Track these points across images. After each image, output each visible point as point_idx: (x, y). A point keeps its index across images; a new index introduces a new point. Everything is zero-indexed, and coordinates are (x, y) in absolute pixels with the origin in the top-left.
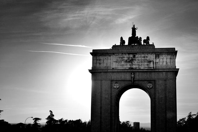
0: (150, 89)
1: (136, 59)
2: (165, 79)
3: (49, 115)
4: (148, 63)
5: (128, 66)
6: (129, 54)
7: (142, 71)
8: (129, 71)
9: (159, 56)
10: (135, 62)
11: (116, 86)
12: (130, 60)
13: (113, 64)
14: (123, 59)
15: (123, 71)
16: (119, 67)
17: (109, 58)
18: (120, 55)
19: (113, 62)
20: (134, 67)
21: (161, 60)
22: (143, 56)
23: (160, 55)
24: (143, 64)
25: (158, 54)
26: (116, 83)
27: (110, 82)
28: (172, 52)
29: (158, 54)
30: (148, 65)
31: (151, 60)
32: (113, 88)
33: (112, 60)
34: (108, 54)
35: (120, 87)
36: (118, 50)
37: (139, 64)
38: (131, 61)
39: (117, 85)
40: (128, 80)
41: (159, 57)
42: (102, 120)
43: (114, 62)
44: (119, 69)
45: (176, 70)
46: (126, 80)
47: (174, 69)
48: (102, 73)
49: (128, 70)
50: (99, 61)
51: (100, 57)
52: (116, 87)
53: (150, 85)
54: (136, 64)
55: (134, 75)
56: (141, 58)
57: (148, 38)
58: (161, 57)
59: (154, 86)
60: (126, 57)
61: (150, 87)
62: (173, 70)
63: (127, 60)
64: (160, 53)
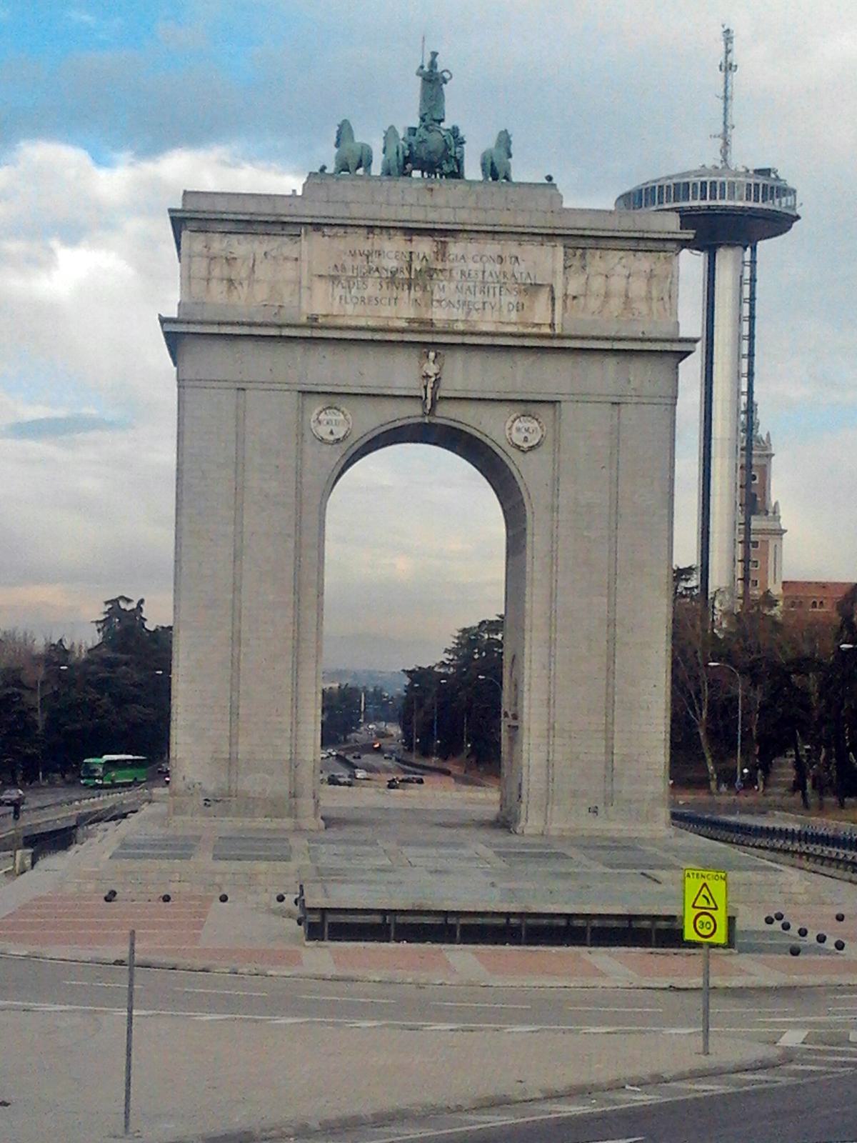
2: (616, 400)
6: (411, 232)
9: (583, 256)
10: (445, 289)
14: (375, 260)
15: (378, 336)
16: (350, 309)
19: (316, 279)
20: (439, 315)
21: (597, 284)
22: (492, 248)
24: (491, 299)
25: (582, 243)
30: (520, 307)
32: (308, 437)
35: (356, 436)
39: (337, 422)
41: (584, 267)
44: (353, 323)
46: (389, 392)
48: (248, 346)
49: (402, 331)
50: (226, 269)
52: (332, 433)
53: (527, 430)
54: (454, 300)
56: (478, 266)
57: (505, 141)
59: (550, 437)
60: (392, 250)
61: (526, 439)
62: (668, 347)
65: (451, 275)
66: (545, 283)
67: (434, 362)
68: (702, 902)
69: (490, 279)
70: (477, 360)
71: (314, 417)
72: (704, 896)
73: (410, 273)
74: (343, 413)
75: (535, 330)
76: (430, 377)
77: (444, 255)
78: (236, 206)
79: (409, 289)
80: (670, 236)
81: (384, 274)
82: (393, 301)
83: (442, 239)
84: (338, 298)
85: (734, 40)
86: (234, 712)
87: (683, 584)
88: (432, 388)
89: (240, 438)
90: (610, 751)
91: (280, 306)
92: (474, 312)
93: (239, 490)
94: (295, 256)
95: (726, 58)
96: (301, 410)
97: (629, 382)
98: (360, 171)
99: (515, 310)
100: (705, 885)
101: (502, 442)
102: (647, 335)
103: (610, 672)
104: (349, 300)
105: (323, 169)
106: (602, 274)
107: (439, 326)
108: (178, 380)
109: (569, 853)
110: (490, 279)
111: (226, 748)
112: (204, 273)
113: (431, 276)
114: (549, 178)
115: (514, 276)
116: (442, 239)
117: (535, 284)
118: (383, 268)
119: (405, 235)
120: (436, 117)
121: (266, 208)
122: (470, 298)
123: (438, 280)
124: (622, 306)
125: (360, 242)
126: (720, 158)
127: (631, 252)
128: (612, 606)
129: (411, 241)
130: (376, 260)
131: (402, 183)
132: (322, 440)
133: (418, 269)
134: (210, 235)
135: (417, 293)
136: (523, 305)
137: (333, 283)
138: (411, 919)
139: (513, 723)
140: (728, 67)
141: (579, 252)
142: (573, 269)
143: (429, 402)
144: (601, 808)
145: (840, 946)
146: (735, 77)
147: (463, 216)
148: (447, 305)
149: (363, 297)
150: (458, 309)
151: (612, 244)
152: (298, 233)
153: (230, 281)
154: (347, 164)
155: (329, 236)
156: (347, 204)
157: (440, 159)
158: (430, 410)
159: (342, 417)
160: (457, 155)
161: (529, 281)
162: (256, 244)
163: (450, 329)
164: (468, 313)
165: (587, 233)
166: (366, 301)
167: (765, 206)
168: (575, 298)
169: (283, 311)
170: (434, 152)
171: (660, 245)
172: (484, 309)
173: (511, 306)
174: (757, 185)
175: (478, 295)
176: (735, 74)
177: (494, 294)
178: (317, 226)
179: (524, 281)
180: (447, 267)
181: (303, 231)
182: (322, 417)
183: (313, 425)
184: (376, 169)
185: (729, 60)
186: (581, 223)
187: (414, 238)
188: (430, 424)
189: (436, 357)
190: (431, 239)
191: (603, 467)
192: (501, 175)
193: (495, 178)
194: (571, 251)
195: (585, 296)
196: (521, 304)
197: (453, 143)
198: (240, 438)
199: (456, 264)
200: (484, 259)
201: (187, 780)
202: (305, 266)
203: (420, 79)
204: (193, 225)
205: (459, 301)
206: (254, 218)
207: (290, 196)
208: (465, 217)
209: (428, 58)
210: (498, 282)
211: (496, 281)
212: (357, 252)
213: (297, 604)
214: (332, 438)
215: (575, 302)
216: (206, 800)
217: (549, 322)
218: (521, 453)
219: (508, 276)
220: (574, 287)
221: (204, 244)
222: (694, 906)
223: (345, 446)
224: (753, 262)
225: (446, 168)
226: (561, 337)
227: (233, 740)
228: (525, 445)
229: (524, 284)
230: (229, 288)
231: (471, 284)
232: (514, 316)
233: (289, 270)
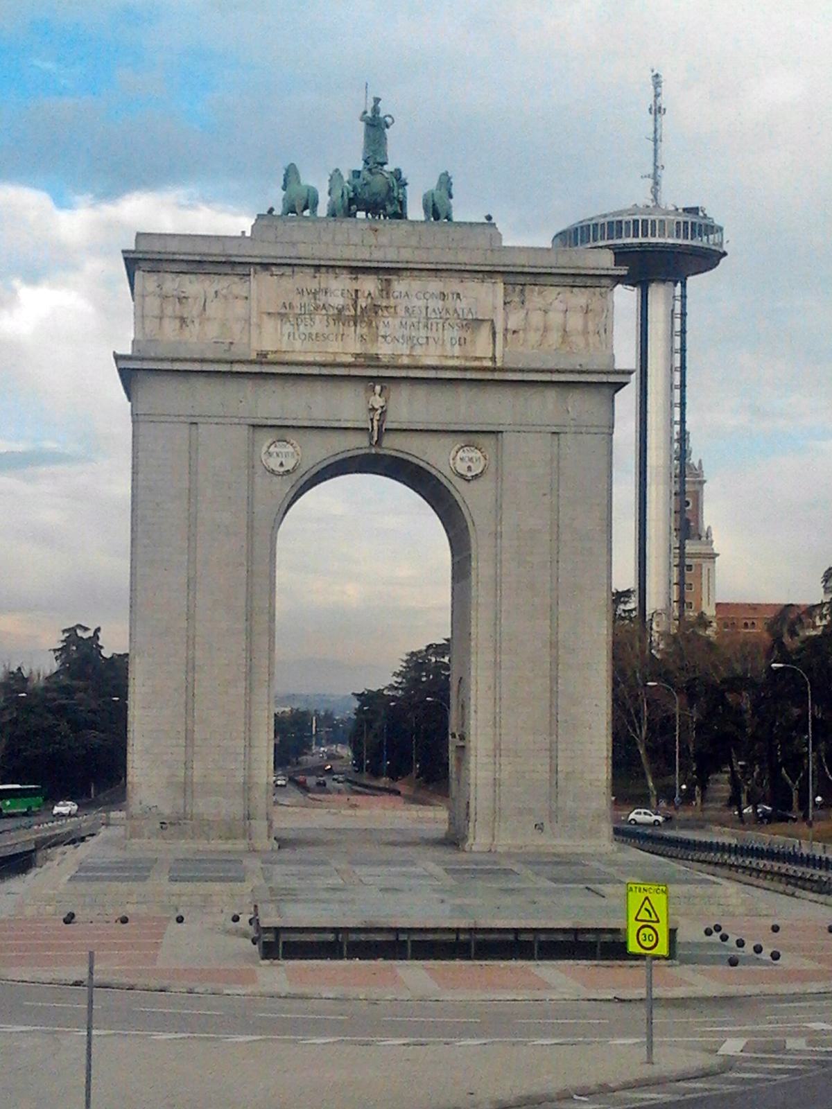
0: (469, 481)
2: (555, 429)
6: (357, 271)
9: (522, 291)
10: (389, 325)
13: (259, 326)
14: (321, 296)
15: (325, 371)
16: (298, 345)
19: (265, 317)
20: (384, 350)
21: (536, 319)
22: (435, 285)
25: (522, 279)
27: (244, 432)
30: (462, 342)
31: (480, 318)
32: (260, 470)
39: (287, 455)
41: (523, 303)
42: (198, 654)
43: (269, 314)
44: (301, 358)
45: (612, 379)
46: (336, 424)
48: (200, 383)
52: (281, 464)
53: (471, 460)
54: (398, 334)
56: (422, 303)
57: (446, 182)
59: (492, 469)
60: (338, 289)
61: (469, 468)
62: (604, 378)
65: (396, 312)
66: (487, 318)
67: (380, 395)
68: (644, 915)
69: (433, 316)
70: (421, 392)
71: (264, 449)
72: (646, 910)
73: (355, 310)
74: (292, 445)
75: (477, 364)
76: (377, 410)
77: (387, 293)
78: (187, 247)
79: (355, 325)
81: (331, 312)
82: (340, 337)
83: (386, 277)
84: (286, 337)
85: (663, 84)
86: (189, 734)
87: (622, 607)
88: (378, 420)
91: (231, 343)
92: (418, 347)
94: (245, 295)
95: (655, 102)
96: (252, 443)
98: (307, 213)
99: (457, 345)
100: (647, 898)
101: (448, 473)
102: (584, 368)
103: (554, 692)
104: (297, 336)
105: (271, 210)
106: (540, 309)
107: (385, 360)
108: (132, 415)
109: (515, 869)
110: (433, 316)
112: (157, 312)
113: (376, 313)
114: (489, 218)
115: (455, 311)
116: (386, 277)
117: (477, 320)
118: (330, 305)
119: (352, 273)
120: (379, 160)
121: (216, 249)
123: (382, 316)
124: (560, 340)
125: (306, 280)
126: (652, 197)
127: (568, 288)
130: (324, 297)
131: (347, 224)
132: (273, 472)
133: (364, 305)
134: (161, 274)
135: (362, 329)
136: (465, 339)
137: (282, 320)
138: (363, 937)
139: (461, 744)
140: (657, 111)
141: (518, 288)
142: (513, 304)
144: (547, 826)
145: (775, 956)
146: (664, 119)
147: (406, 254)
148: (392, 341)
150: (403, 344)
152: (248, 273)
153: (183, 320)
154: (294, 206)
155: (277, 275)
156: (294, 244)
157: (383, 200)
158: (377, 441)
159: (290, 449)
160: (401, 196)
163: (395, 364)
165: (526, 270)
166: (314, 337)
167: (694, 243)
168: (514, 332)
169: (233, 348)
170: (378, 194)
171: (595, 282)
172: (427, 343)
173: (454, 342)
174: (686, 223)
175: (421, 330)
176: (664, 117)
177: (437, 330)
178: (266, 266)
179: (465, 317)
180: (392, 305)
181: (252, 270)
182: (272, 449)
184: (322, 210)
185: (658, 104)
186: (521, 260)
187: (359, 276)
188: (377, 455)
189: (382, 391)
190: (376, 277)
191: (545, 495)
192: (443, 216)
193: (437, 218)
194: (510, 287)
195: (525, 330)
196: (462, 341)
197: (395, 184)
199: (399, 300)
200: (427, 296)
201: (144, 803)
202: (254, 304)
203: (363, 124)
204: (146, 266)
205: (403, 336)
206: (205, 259)
207: (239, 237)
208: (407, 255)
210: (441, 318)
211: (438, 316)
212: (305, 290)
213: (249, 632)
214: (282, 470)
215: (515, 335)
216: (163, 823)
217: (490, 355)
218: (466, 482)
219: (451, 312)
220: (515, 321)
221: (156, 284)
222: (636, 919)
223: (294, 477)
224: (684, 296)
225: (390, 209)
226: (502, 370)
227: (187, 765)
228: (469, 474)
229: (465, 319)
230: (181, 326)
231: (414, 320)
232: (457, 350)
233: (239, 308)
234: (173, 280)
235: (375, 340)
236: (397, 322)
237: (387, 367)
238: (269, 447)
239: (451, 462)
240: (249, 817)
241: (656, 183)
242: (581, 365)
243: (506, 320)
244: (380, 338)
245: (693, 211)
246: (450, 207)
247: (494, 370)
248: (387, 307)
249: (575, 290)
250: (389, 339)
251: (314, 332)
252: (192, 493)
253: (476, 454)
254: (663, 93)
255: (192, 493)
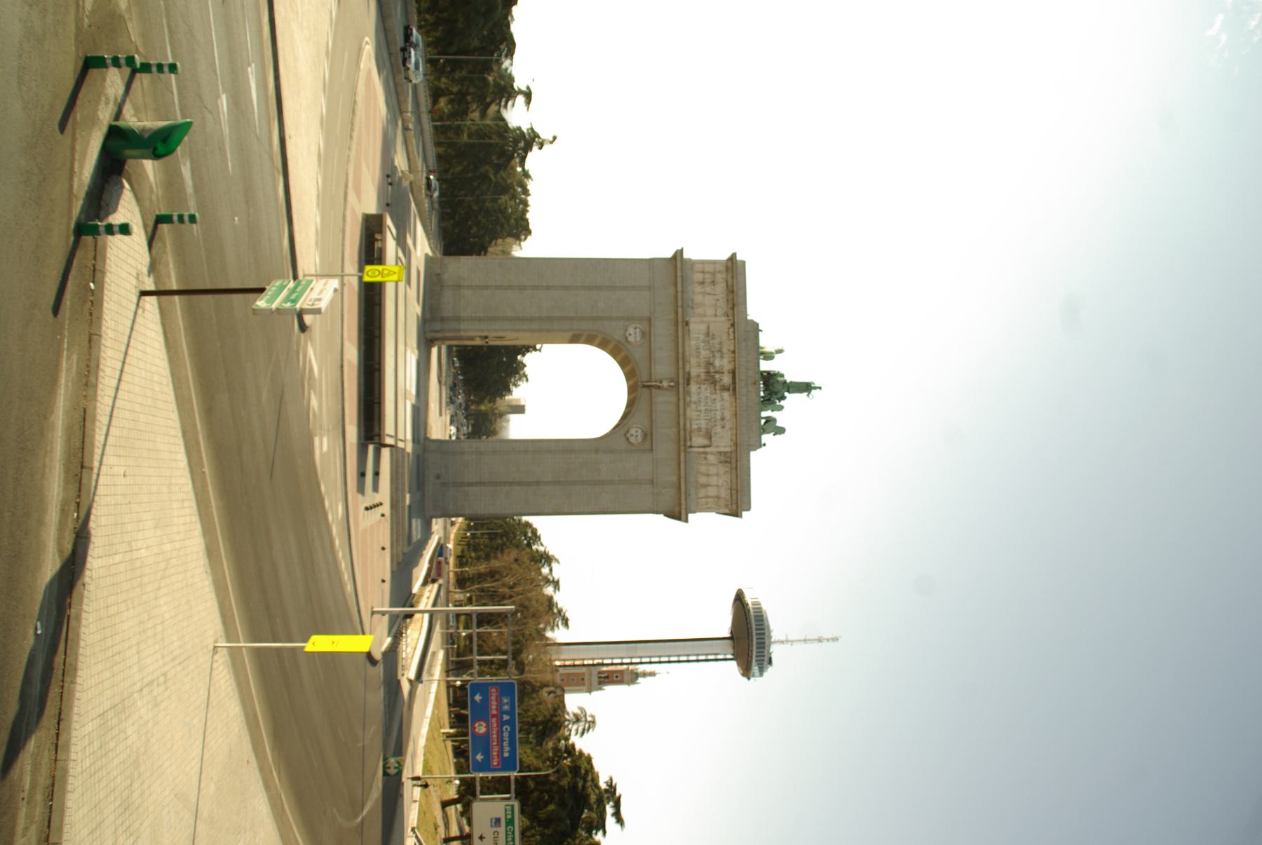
0: (625, 435)
1: (715, 393)
2: (655, 481)
3: (541, 135)
4: (703, 430)
5: (696, 370)
6: (733, 372)
7: (681, 412)
8: (681, 371)
9: (726, 462)
10: (706, 391)
11: (634, 334)
12: (713, 377)
13: (702, 322)
14: (718, 355)
15: (680, 356)
16: (693, 342)
17: (720, 312)
18: (728, 346)
19: (707, 325)
20: (693, 388)
21: (713, 470)
22: (728, 414)
23: (729, 465)
25: (733, 461)
26: (643, 334)
28: (737, 504)
29: (733, 461)
30: (699, 429)
31: (713, 439)
33: (715, 322)
34: (733, 308)
36: (745, 340)
37: (700, 402)
38: (711, 378)
39: (636, 337)
40: (653, 370)
41: (721, 462)
43: (708, 327)
44: (687, 344)
47: (686, 509)
48: (672, 291)
49: (684, 369)
50: (708, 281)
51: (724, 285)
52: (630, 335)
53: (637, 436)
54: (702, 395)
55: (666, 389)
56: (718, 407)
57: (781, 431)
58: (722, 469)
60: (723, 363)
61: (632, 435)
62: (683, 507)
63: (714, 367)
64: (734, 465)
65: (713, 394)
69: (712, 414)
71: (638, 326)
75: (688, 438)
79: (706, 372)
80: (739, 505)
81: (711, 360)
86: (486, 287)
87: (560, 623)
89: (625, 288)
90: (470, 484)
91: (692, 308)
93: (599, 288)
96: (641, 319)
97: (664, 488)
103: (512, 484)
110: (712, 414)
111: (466, 284)
112: (706, 270)
113: (712, 383)
114: (764, 445)
115: (715, 426)
122: (703, 404)
126: (777, 640)
128: (546, 483)
129: (729, 373)
132: (626, 330)
135: (703, 376)
140: (820, 640)
143: (649, 384)
147: (744, 399)
149: (698, 349)
151: (734, 476)
159: (638, 339)
161: (713, 434)
162: (723, 295)
164: (695, 403)
167: (754, 660)
168: (705, 458)
170: (773, 387)
178: (733, 325)
182: (638, 330)
183: (634, 325)
189: (672, 386)
191: (619, 476)
195: (707, 464)
198: (625, 288)
199: (719, 396)
209: (817, 385)
213: (540, 319)
214: (627, 334)
217: (693, 445)
220: (711, 458)
224: (725, 659)
227: (470, 287)
232: (695, 427)
233: (710, 312)
234: (722, 279)
235: (698, 383)
236: (708, 395)
237: (684, 387)
238: (639, 328)
239: (634, 426)
240: (442, 320)
241: (782, 642)
242: (689, 495)
243: (712, 453)
244: (698, 386)
245: (770, 662)
246: (769, 433)
247: (685, 445)
248: (715, 389)
249: (729, 491)
250: (699, 390)
251: (701, 350)
252: (612, 288)
253: (640, 439)
254: (828, 643)
255: (612, 288)
